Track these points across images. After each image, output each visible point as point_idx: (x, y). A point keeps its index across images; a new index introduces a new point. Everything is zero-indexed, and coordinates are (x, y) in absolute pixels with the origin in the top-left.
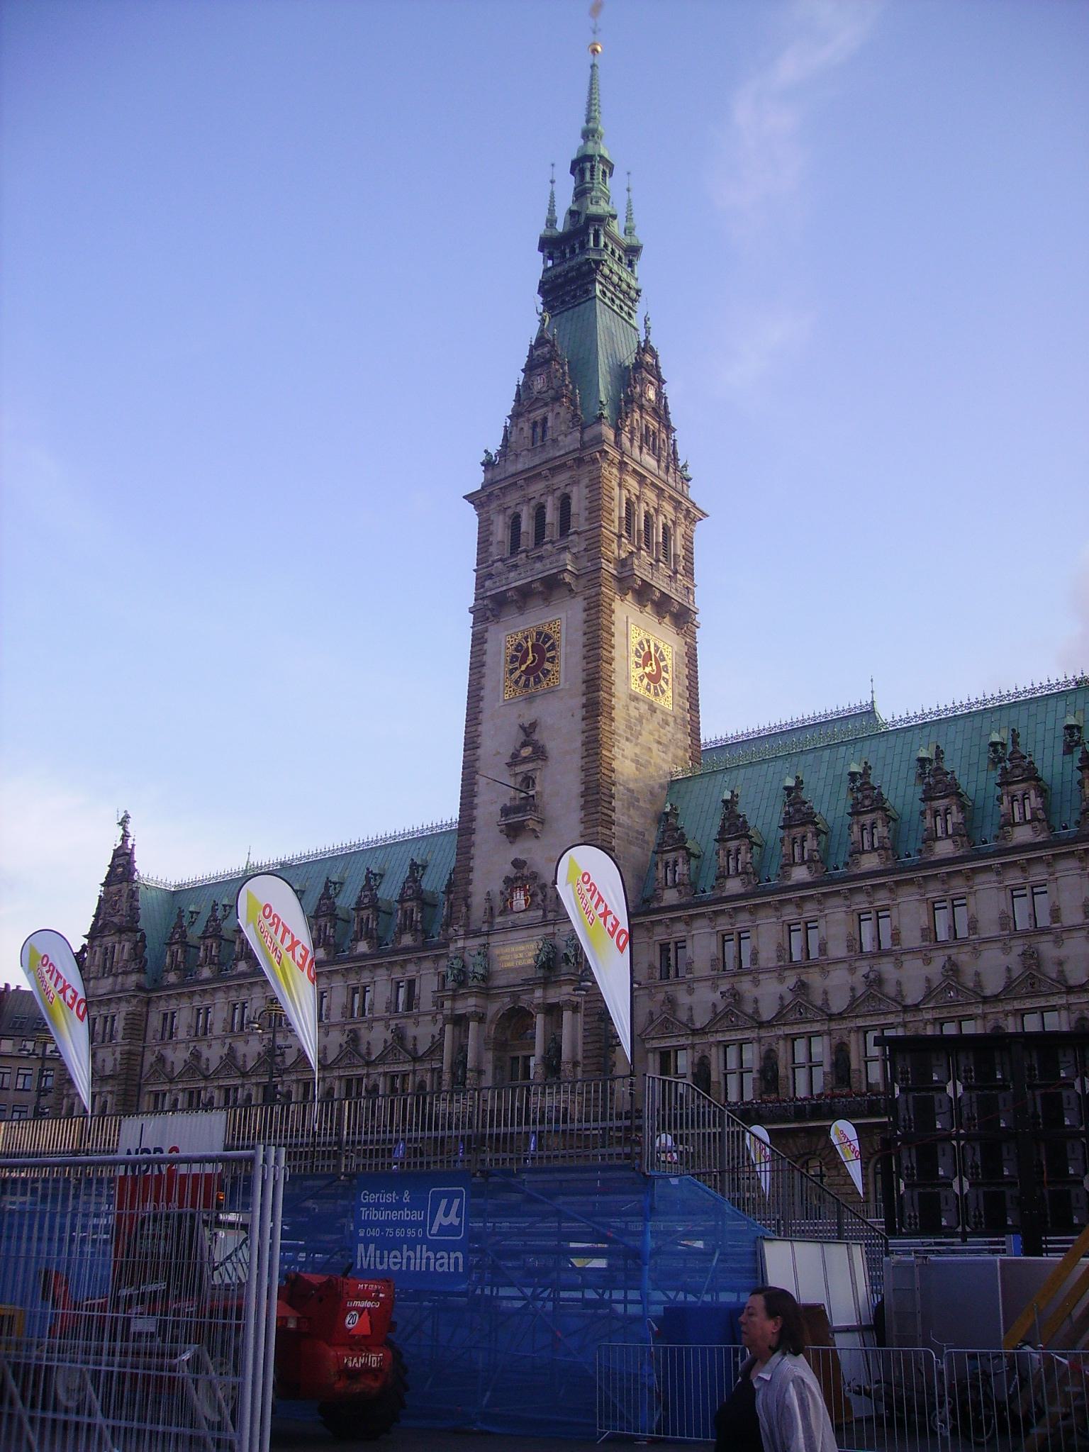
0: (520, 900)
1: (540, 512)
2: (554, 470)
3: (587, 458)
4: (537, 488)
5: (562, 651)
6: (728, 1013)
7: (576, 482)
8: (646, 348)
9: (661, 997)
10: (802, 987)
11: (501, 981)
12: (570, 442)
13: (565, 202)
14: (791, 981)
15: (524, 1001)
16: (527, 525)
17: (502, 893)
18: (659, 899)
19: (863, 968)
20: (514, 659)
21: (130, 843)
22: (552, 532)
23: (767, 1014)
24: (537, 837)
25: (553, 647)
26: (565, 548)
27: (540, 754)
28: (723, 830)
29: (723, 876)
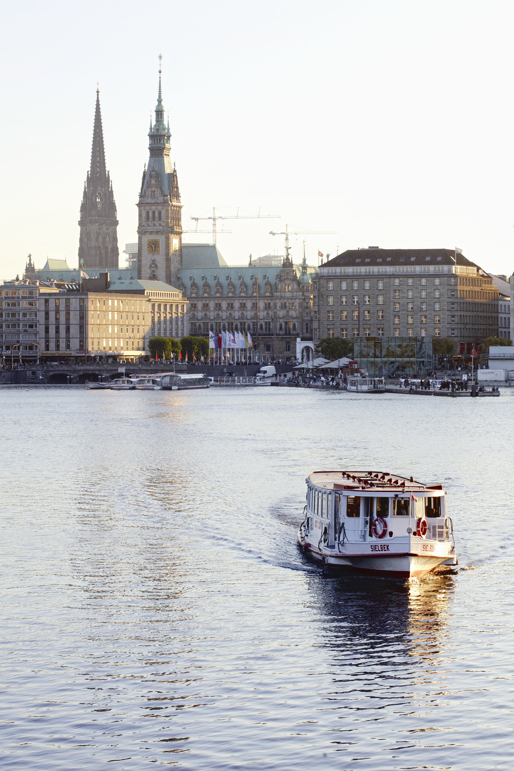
1: (154, 212)
2: (157, 205)
4: (153, 208)
5: (160, 246)
6: (193, 318)
8: (175, 171)
10: (206, 314)
12: (161, 199)
13: (154, 123)
14: (204, 313)
16: (151, 215)
19: (216, 312)
21: (32, 262)
23: (200, 318)
25: (158, 245)
26: (160, 225)
27: (156, 266)
28: (192, 285)
29: (192, 293)
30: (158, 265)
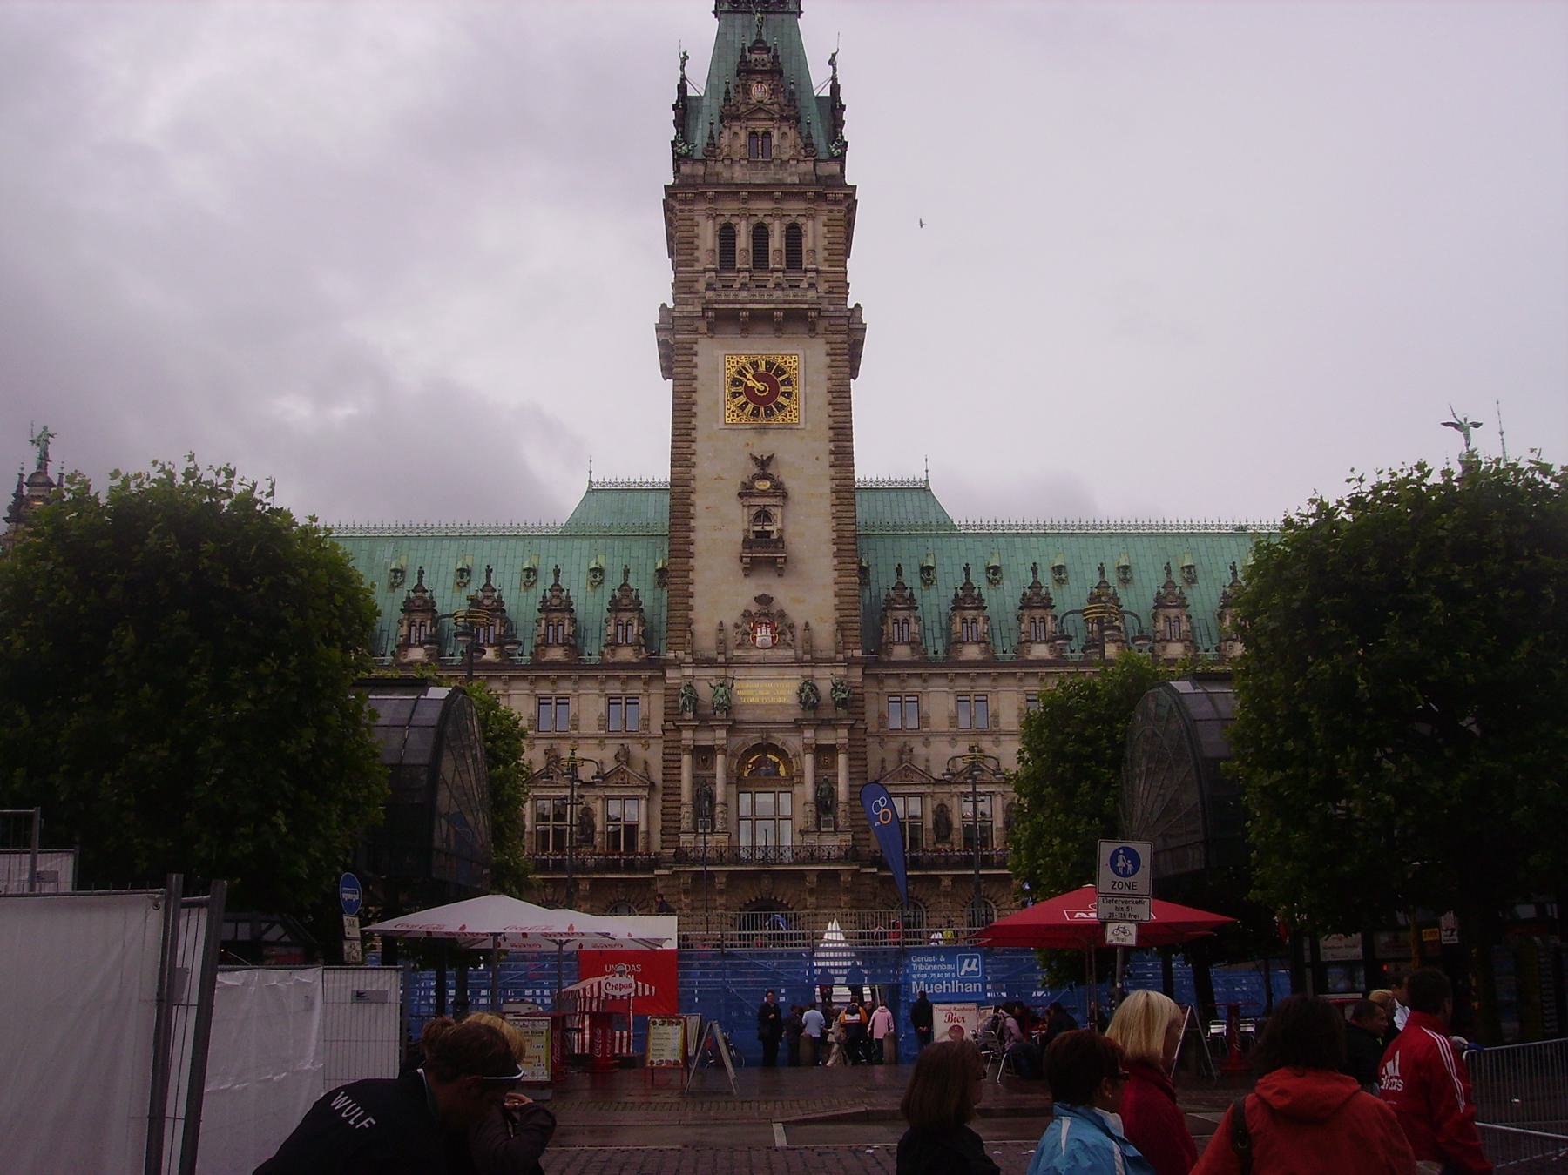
0: (763, 635)
2: (787, 196)
3: (831, 197)
4: (762, 207)
5: (800, 390)
7: (811, 216)
9: (894, 745)
11: (746, 716)
15: (778, 738)
16: (743, 241)
17: (737, 626)
18: (889, 653)
20: (735, 382)
22: (776, 259)
24: (780, 573)
27: (780, 491)
30: (790, 484)
